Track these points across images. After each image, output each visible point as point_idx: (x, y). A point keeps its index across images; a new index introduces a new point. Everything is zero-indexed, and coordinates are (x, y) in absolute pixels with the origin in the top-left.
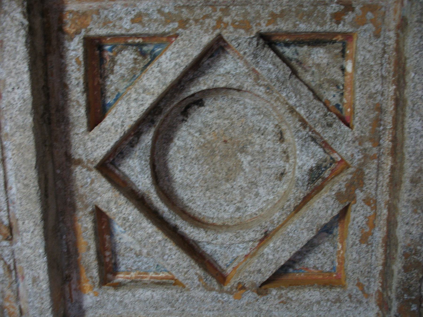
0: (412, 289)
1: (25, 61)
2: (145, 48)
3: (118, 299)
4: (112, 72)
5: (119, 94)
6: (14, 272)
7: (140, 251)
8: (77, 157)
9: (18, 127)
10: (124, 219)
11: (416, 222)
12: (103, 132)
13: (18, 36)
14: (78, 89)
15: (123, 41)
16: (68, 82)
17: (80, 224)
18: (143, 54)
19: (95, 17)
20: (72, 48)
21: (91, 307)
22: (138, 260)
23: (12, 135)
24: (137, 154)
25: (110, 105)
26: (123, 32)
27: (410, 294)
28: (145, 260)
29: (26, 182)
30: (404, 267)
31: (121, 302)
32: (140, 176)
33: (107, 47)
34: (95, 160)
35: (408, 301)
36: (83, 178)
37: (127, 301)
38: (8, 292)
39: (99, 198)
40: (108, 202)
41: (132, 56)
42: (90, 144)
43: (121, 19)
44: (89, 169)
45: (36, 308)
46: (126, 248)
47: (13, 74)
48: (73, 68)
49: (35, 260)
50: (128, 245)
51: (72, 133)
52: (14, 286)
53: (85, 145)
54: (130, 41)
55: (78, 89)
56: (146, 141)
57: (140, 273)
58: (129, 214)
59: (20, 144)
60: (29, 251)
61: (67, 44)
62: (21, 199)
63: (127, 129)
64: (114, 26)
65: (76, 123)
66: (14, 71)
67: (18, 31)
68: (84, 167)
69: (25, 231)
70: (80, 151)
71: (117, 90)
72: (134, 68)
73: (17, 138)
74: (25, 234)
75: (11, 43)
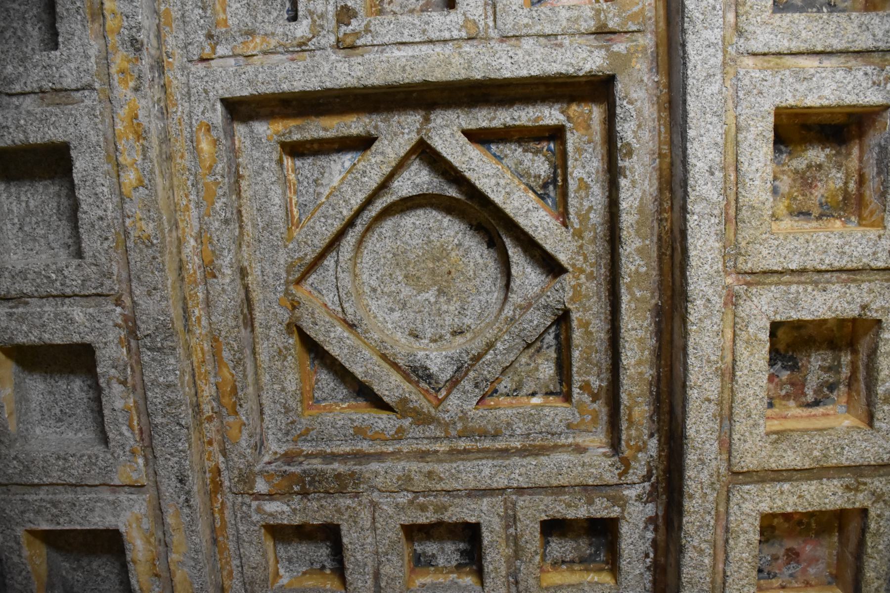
0: (317, 484)
2: (551, 187)
3: (267, 164)
4: (525, 151)
5: (502, 159)
6: (299, 49)
7: (322, 184)
8: (432, 117)
10: (364, 172)
11: (388, 481)
12: (461, 148)
13: (568, 65)
14: (508, 119)
15: (560, 163)
16: (515, 108)
17: (355, 119)
18: (545, 186)
19: (585, 139)
20: (553, 112)
21: (253, 132)
22: (310, 182)
23: (460, 54)
24: (435, 179)
25: (489, 149)
26: (570, 170)
27: (310, 483)
28: (311, 190)
29: (408, 68)
30: (339, 474)
31: (263, 168)
32: (409, 182)
33: (552, 145)
34: (429, 138)
35: (303, 481)
36: (408, 124)
37: (265, 175)
38: (273, 42)
39: (387, 143)
40: (382, 153)
41: (543, 174)
42: (448, 132)
43: (584, 167)
44: (419, 132)
45: (256, 76)
46: (323, 167)
47: (527, 57)
48: (532, 114)
49: (316, 76)
50: (327, 170)
51: (459, 111)
52: (280, 50)
53: (448, 126)
54: (559, 171)
55: (508, 119)
56: (450, 190)
57: (294, 185)
58: (370, 177)
59: (450, 64)
60: (326, 70)
61: (557, 106)
62: (388, 62)
63: (466, 174)
64: (576, 160)
65: (471, 116)
66: (530, 59)
68: (421, 124)
69: (350, 66)
70: (439, 121)
71: (506, 156)
72: (529, 175)
73: (456, 60)
74: (346, 65)
75: (560, 57)
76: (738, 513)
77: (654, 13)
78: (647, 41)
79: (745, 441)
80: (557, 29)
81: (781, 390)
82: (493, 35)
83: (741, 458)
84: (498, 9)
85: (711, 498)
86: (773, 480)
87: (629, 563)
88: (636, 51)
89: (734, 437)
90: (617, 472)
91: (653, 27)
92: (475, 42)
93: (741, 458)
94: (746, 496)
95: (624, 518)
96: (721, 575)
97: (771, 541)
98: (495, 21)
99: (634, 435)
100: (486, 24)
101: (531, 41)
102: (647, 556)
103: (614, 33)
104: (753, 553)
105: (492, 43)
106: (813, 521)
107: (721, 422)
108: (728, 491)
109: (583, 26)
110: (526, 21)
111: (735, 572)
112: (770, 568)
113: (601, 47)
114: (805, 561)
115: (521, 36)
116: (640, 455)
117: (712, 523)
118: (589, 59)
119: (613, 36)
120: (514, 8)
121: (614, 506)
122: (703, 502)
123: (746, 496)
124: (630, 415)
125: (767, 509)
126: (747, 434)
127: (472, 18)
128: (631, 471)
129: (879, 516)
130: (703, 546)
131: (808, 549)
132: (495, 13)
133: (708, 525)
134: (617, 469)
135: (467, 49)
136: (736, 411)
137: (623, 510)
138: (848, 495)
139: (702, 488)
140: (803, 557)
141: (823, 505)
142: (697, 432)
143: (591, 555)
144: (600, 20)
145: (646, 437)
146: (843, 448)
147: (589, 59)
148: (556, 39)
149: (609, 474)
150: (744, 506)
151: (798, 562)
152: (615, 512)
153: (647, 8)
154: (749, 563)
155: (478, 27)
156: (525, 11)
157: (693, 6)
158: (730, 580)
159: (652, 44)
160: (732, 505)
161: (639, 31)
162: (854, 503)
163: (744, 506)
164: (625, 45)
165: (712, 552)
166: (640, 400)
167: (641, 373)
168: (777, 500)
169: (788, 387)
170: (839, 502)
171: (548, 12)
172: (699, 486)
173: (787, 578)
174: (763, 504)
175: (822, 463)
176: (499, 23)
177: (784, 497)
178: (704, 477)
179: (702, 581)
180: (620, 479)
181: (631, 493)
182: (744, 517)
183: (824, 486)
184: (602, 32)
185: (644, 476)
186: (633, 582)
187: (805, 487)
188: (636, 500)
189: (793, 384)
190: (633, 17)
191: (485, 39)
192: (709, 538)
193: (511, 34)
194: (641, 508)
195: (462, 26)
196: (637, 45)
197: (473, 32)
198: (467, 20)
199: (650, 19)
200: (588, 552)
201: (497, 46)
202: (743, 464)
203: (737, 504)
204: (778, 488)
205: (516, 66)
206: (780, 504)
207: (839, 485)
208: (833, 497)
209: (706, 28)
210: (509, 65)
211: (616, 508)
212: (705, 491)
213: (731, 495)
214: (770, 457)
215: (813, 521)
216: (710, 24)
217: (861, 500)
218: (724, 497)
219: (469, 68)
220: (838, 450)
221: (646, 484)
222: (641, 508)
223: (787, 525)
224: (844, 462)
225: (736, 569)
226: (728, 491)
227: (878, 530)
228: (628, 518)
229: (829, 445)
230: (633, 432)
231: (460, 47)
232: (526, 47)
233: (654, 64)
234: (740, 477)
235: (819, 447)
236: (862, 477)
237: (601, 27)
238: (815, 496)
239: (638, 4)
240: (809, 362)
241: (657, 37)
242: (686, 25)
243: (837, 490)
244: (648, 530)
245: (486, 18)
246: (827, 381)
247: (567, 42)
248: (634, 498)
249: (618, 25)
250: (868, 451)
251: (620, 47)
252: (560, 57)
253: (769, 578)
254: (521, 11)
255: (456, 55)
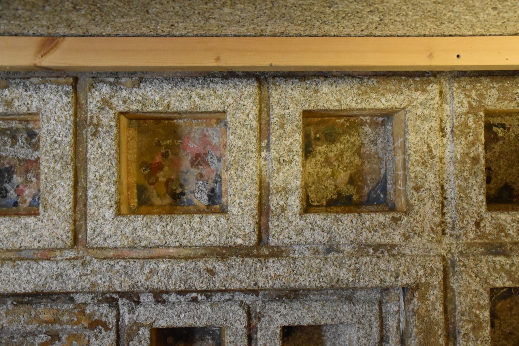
76: (114, 238)
79: (41, 236)
81: (32, 182)
83: (58, 238)
85: (98, 265)
86: (85, 205)
87: (199, 318)
89: (36, 247)
90: (104, 333)
93: (58, 238)
94: (98, 230)
95: (151, 325)
96: (181, 249)
97: (182, 182)
99: (68, 318)
102: (194, 300)
104: (157, 221)
106: (164, 143)
107: (22, 259)
108: (92, 248)
111: (176, 238)
112: (211, 182)
114: (204, 148)
116: (88, 312)
117: (123, 263)
121: (138, 334)
122: (100, 273)
123: (98, 230)
124: (47, 322)
125: (111, 210)
126: (34, 234)
128: (104, 319)
129: (125, 102)
130: (147, 271)
131: (193, 146)
133: (125, 267)
134: (100, 332)
136: (10, 246)
137: (143, 325)
138: (102, 133)
139: (86, 275)
140: (201, 151)
141: (111, 157)
142: (28, 282)
143: (213, 339)
145: (71, 306)
146: (56, 141)
149: (105, 340)
150: (107, 233)
151: (206, 154)
152: (145, 333)
154: (167, 224)
158: (185, 242)
160: (106, 245)
162: (111, 127)
163: (107, 233)
165: (154, 261)
166: (33, 313)
167: (7, 314)
168: (103, 202)
169: (29, 175)
170: (109, 141)
172: (84, 278)
173: (222, 163)
174: (107, 214)
175: (69, 160)
177: (100, 194)
178: (74, 273)
179: (184, 270)
180: (110, 329)
181: (127, 318)
182: (119, 233)
183: (92, 156)
185: (110, 307)
186: (220, 314)
187: (91, 176)
188: (134, 313)
189: (27, 172)
192: (138, 265)
194: (142, 308)
200: (210, 342)
202: (64, 237)
203: (105, 239)
204: (91, 201)
206: (107, 198)
207: (92, 142)
208: (103, 148)
211: (140, 332)
212: (89, 272)
213: (95, 246)
214: (59, 210)
215: (164, 143)
217: (107, 119)
218: (99, 252)
220: (57, 146)
221: (120, 302)
222: (142, 308)
223: (166, 168)
224: (68, 139)
225: (173, 237)
226: (92, 248)
227: (139, 102)
228: (151, 321)
229: (51, 155)
230: (65, 318)
234: (80, 237)
235: (52, 165)
236: (86, 121)
238: (101, 165)
240: (6, 157)
243: (97, 144)
244: (168, 299)
246: (26, 139)
248: (131, 316)
250: (59, 117)
253: (220, 181)
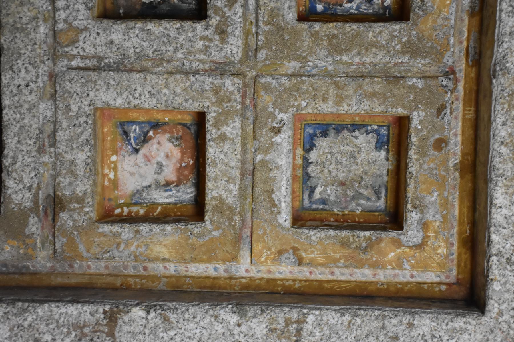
1: (6, 123)
9: (23, 30)
13: (14, 158)
23: (35, 18)
47: (26, 106)
67: (14, 163)
73: (27, 13)
75: (24, 148)
77: (77, 271)
78: (42, 261)
80: (62, 148)
82: (60, 64)
84: (90, 73)
88: (27, 246)
91: (60, 270)
92: (50, 41)
98: (78, 68)
100: (74, 57)
101: (49, 114)
103: (54, 220)
105: (49, 63)
109: (64, 181)
110: (74, 108)
113: (36, 202)
115: (55, 100)
118: (21, 186)
119: (50, 218)
120: (92, 94)
127: (81, 38)
132: (87, 69)
135: (42, 29)
144: (71, 202)
147: (21, 186)
148: (50, 146)
153: (84, 263)
155: (67, 46)
156: (87, 108)
157: (41, 314)
159: (39, 268)
161: (55, 251)
164: (39, 232)
171: (83, 137)
176: (73, 73)
184: (56, 204)
190: (72, 244)
191: (54, 54)
193: (58, 88)
195: (70, 24)
196: (35, 247)
197: (63, 39)
198: (79, 31)
199: (71, 266)
201: (43, 69)
205: (15, 91)
209: (11, 330)
210: (16, 82)
216: (16, 335)
219: (15, 29)
231: (45, 20)
232: (42, 106)
233: (12, 270)
237: (61, 202)
239: (88, 251)
241: (46, 274)
242: (20, 304)
245: (82, 57)
247: (46, 159)
249: (62, 225)
251: (34, 226)
252: (24, 148)
254: (86, 103)
255: (33, 14)
